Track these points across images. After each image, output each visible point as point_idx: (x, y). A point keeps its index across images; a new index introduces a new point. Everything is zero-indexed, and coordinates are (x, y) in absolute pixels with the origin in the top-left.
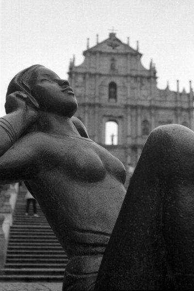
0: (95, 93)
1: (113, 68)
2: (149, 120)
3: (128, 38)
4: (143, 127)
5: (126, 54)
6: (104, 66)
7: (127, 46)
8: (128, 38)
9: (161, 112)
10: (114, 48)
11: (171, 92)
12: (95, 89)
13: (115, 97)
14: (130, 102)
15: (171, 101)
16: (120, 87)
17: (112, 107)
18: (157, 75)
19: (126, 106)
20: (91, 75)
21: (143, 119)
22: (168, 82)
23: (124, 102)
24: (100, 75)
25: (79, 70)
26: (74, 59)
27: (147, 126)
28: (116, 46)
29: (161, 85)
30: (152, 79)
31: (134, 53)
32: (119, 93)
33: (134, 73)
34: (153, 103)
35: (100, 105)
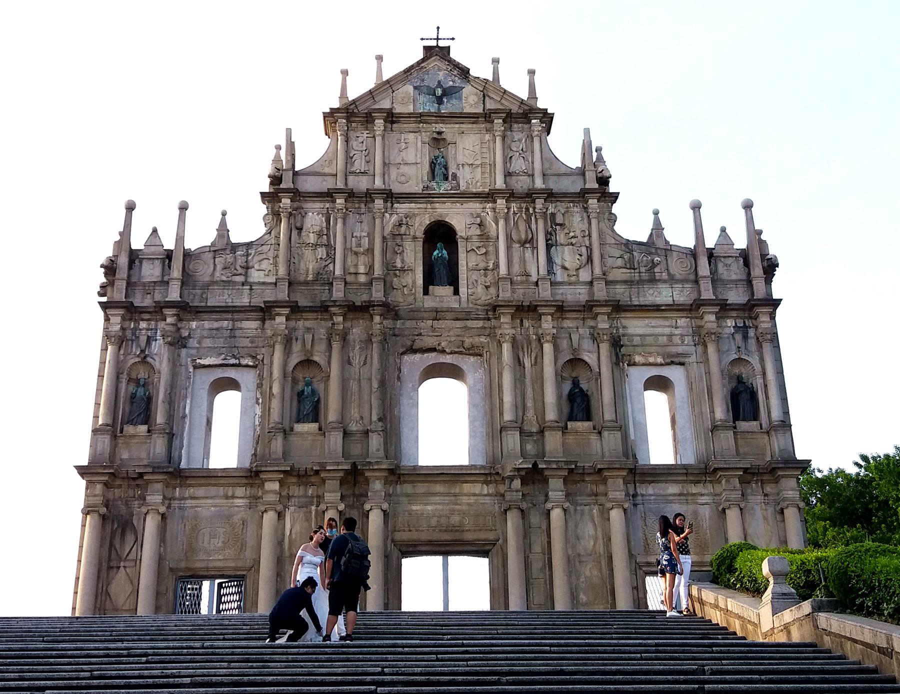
0: (371, 267)
1: (439, 168)
2: (590, 358)
3: (496, 61)
4: (567, 387)
5: (487, 117)
6: (407, 160)
7: (489, 88)
8: (496, 61)
9: (636, 327)
10: (439, 100)
11: (669, 249)
12: (370, 251)
13: (454, 282)
14: (506, 294)
15: (672, 280)
16: (467, 239)
17: (437, 314)
18: (612, 188)
19: (494, 308)
20: (351, 195)
21: (566, 356)
22: (656, 213)
23: (484, 296)
24: (390, 196)
25: (309, 185)
26: (291, 146)
27: (584, 385)
28: (449, 92)
29: (632, 225)
30: (593, 202)
31: (515, 109)
32: (465, 262)
33: (521, 184)
34: (600, 292)
35: (390, 310)
